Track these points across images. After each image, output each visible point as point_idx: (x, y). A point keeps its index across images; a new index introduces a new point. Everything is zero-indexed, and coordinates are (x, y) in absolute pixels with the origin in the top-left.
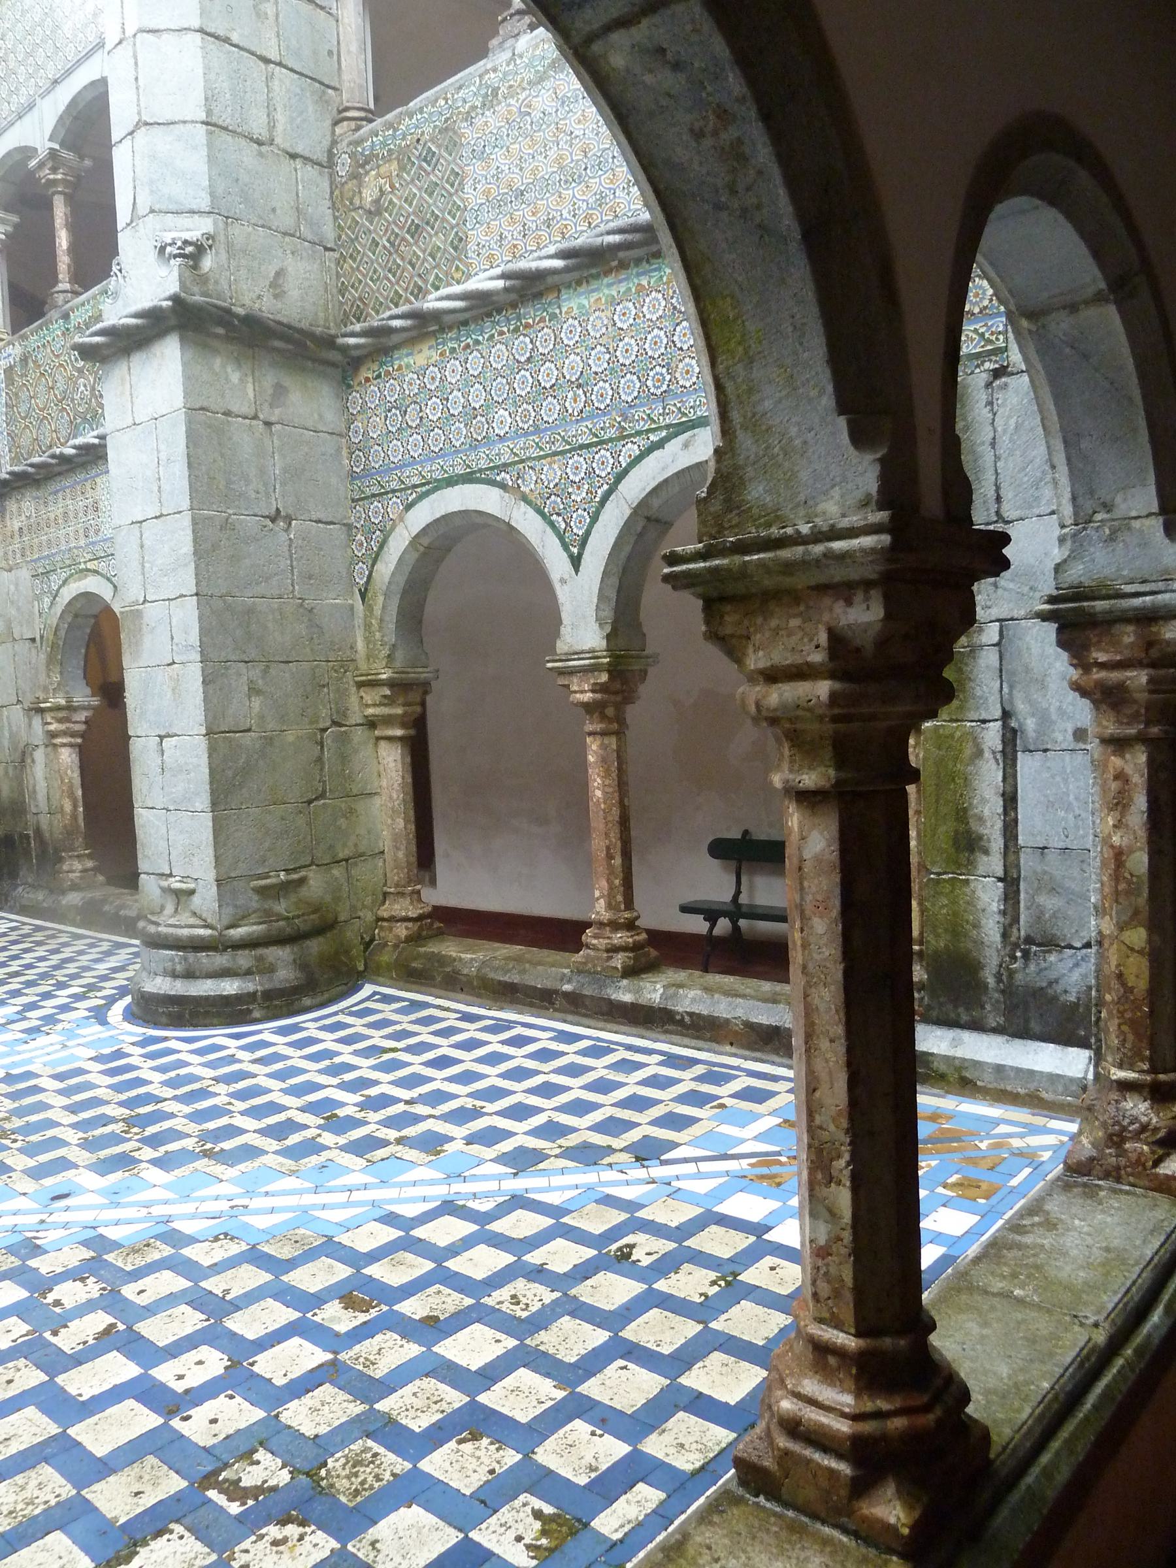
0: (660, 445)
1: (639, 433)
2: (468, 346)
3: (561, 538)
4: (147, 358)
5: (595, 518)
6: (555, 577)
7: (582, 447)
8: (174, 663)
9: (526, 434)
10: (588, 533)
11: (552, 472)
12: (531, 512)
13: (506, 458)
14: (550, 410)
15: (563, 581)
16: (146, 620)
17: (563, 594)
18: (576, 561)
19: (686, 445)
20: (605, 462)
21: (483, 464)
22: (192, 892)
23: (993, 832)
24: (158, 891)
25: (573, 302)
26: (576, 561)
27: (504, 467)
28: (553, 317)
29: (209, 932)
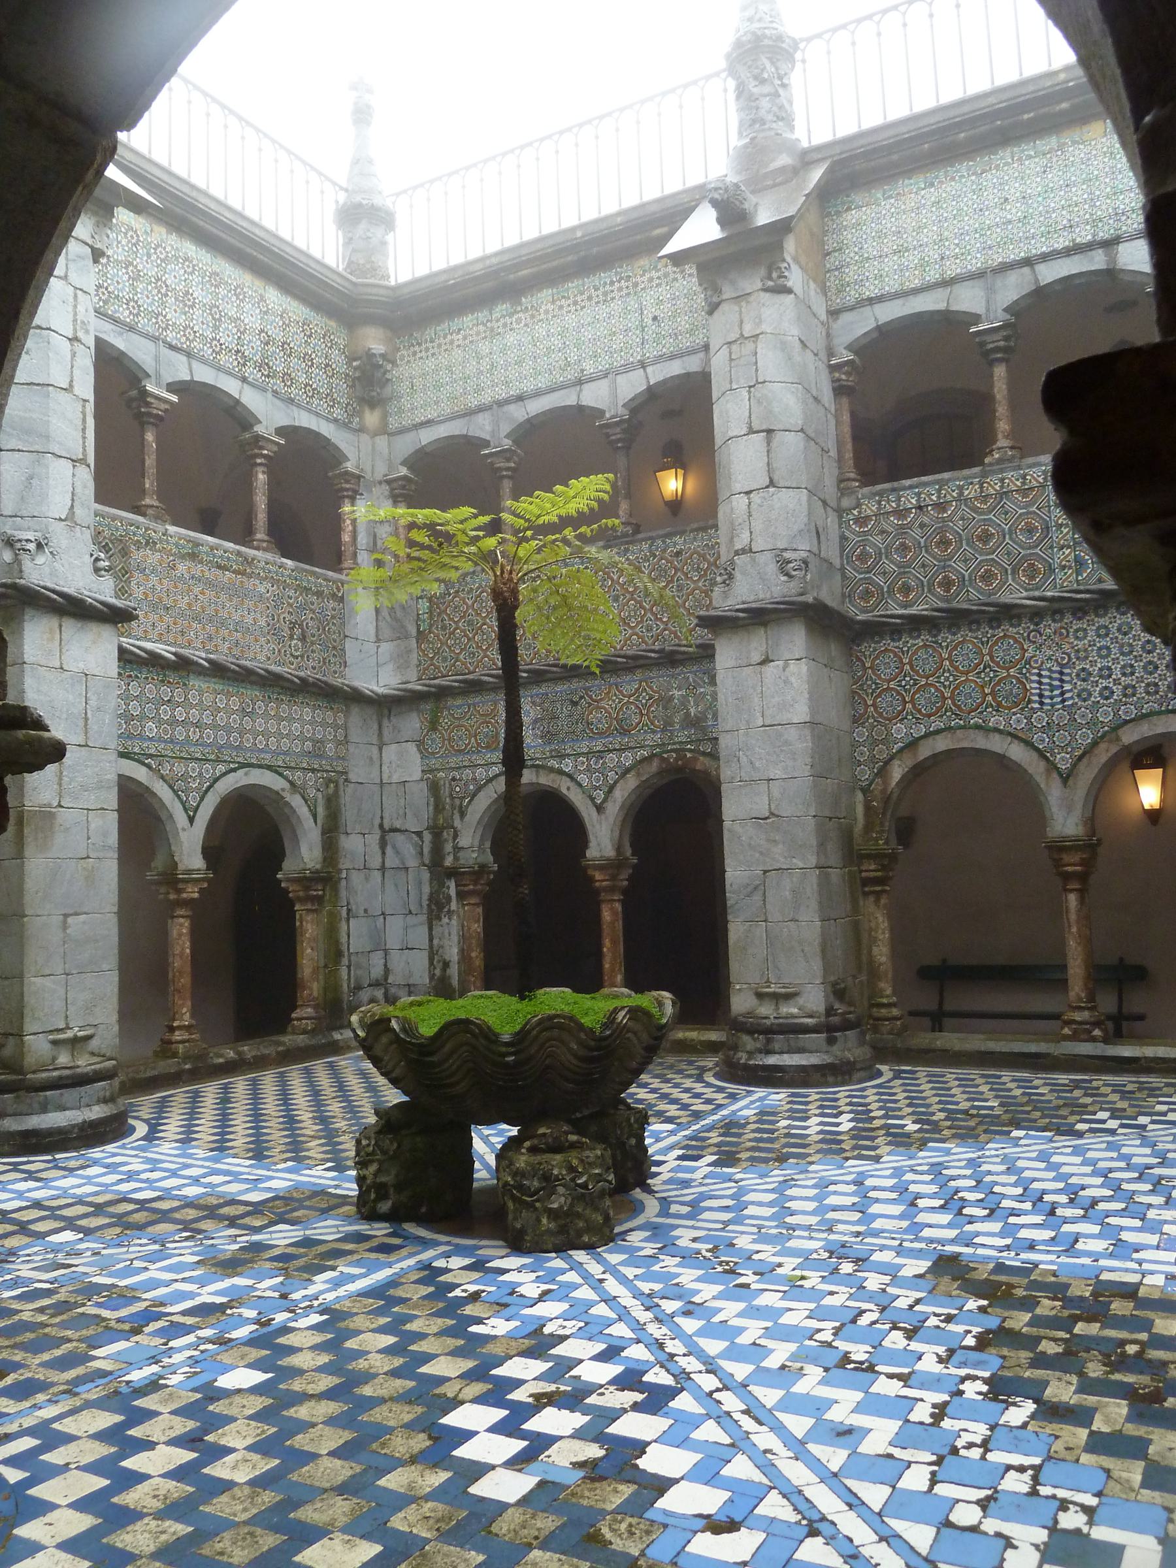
0: (234, 770)
1: (225, 761)
2: (130, 676)
3: (183, 804)
4: (82, 628)
5: (202, 799)
6: (179, 826)
7: (197, 759)
8: (88, 857)
9: (165, 741)
10: (198, 806)
11: (179, 768)
12: (166, 787)
13: (152, 751)
14: (180, 733)
15: (184, 829)
16: (59, 820)
17: (183, 836)
18: (191, 820)
19: (246, 774)
20: (209, 771)
21: (136, 750)
22: (89, 1038)
23: (344, 948)
24: (49, 1045)
25: (195, 682)
26: (191, 820)
27: (151, 756)
28: (185, 684)
29: (114, 1062)
